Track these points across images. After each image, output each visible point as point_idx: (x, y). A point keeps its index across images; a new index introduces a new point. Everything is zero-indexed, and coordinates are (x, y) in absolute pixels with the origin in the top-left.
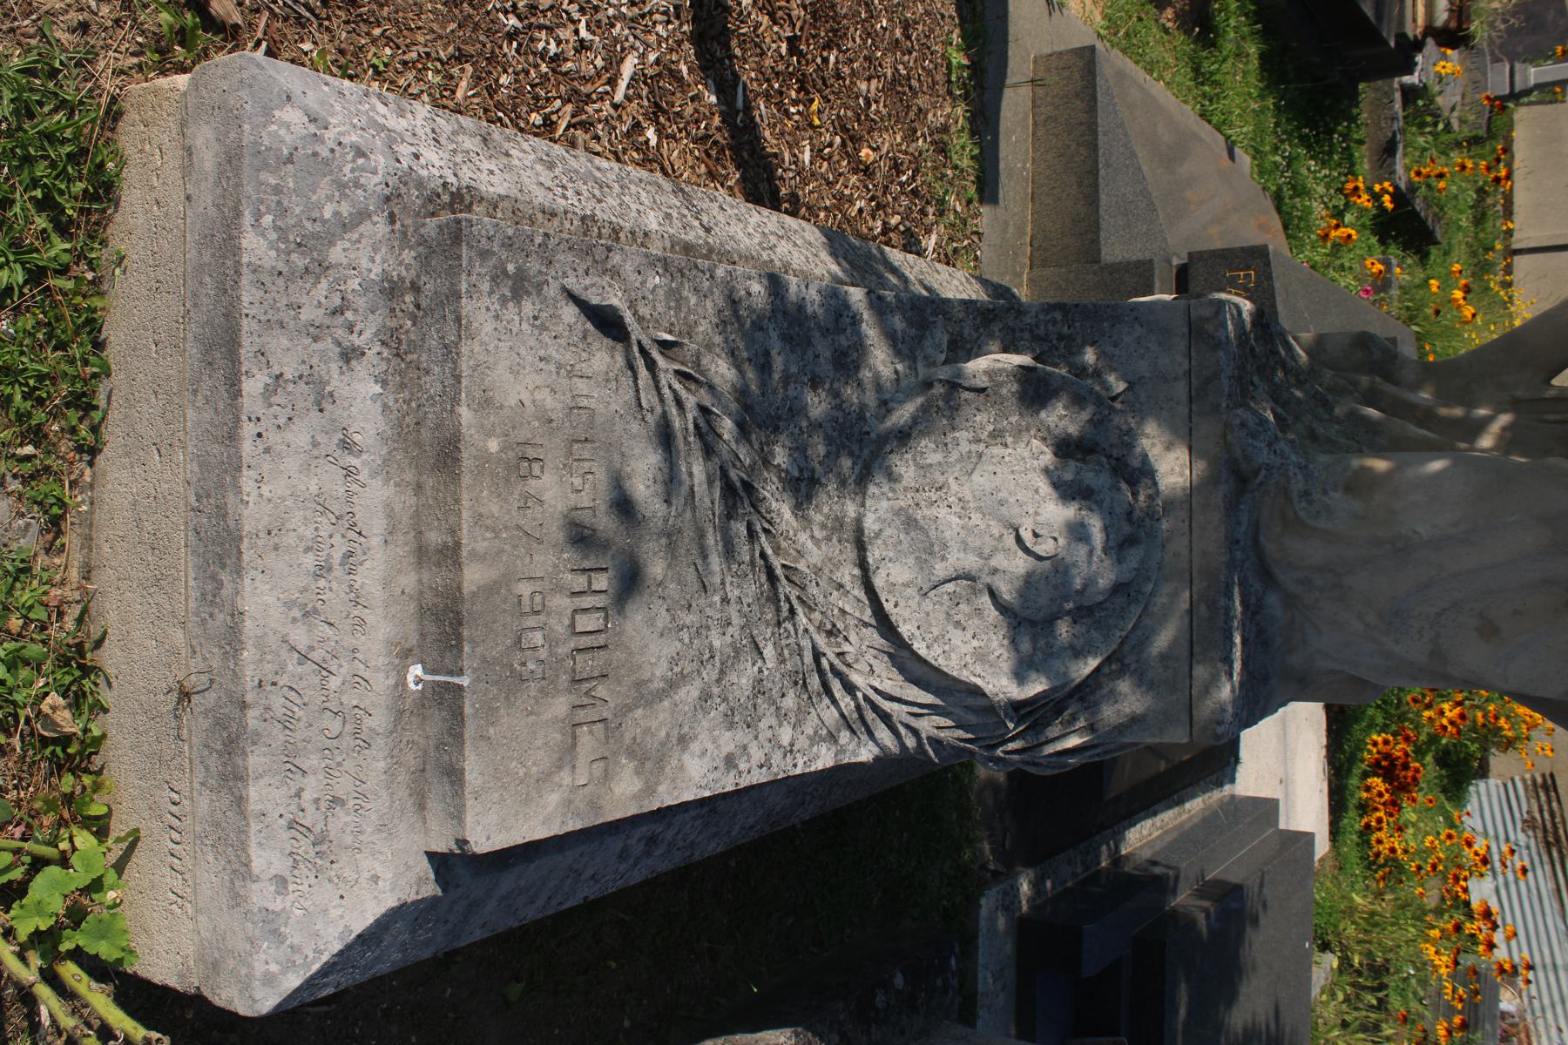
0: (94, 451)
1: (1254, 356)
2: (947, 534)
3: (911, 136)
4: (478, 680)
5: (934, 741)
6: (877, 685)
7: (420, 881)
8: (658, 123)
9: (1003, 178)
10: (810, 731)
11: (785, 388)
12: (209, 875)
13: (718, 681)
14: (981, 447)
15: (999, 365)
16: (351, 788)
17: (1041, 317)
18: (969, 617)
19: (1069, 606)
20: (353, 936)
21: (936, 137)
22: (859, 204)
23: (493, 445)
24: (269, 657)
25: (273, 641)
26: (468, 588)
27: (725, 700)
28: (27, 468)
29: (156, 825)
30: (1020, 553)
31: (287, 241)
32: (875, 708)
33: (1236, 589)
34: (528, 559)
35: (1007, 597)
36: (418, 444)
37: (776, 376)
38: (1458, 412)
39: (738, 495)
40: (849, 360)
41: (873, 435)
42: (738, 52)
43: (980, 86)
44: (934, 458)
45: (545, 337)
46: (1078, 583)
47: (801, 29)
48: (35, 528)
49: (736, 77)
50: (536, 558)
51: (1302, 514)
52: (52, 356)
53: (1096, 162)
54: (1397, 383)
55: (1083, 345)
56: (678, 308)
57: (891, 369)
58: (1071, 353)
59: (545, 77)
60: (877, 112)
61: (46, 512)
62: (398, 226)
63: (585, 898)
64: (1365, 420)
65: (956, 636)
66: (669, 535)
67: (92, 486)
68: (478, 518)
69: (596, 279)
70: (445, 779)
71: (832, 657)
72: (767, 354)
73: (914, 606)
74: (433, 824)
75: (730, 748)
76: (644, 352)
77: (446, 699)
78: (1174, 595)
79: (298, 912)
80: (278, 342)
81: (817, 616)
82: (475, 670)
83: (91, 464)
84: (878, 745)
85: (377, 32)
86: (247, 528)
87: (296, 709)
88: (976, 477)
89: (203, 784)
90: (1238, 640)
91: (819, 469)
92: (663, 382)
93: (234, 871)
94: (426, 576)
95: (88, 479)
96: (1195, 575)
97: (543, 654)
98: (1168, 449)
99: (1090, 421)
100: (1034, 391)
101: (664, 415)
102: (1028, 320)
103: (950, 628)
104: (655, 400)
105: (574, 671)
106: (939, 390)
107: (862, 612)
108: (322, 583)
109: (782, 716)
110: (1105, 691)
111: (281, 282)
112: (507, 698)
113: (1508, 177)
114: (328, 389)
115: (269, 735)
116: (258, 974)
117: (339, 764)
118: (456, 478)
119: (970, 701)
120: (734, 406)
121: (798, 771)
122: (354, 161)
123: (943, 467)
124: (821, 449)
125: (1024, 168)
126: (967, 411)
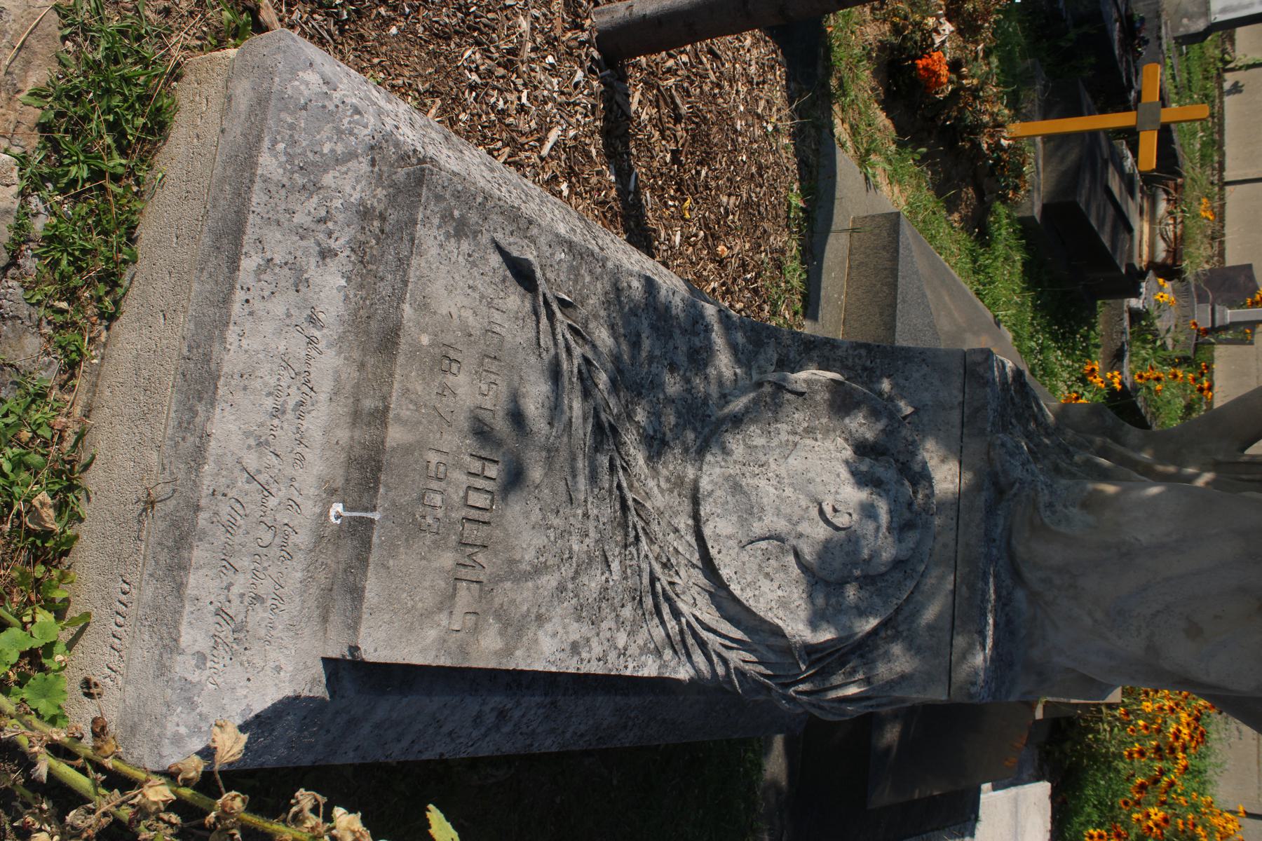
0: (112, 318)
1: (1014, 404)
2: (765, 500)
3: (756, 248)
4: (385, 518)
5: (741, 673)
6: (698, 614)
7: (314, 681)
8: (570, 182)
9: (822, 302)
10: (641, 642)
11: (650, 366)
12: (141, 651)
13: (573, 579)
14: (797, 438)
16: (271, 590)
19: (857, 573)
20: (252, 714)
21: (775, 255)
22: (713, 285)
23: (425, 340)
24: (224, 473)
25: (229, 460)
26: (389, 443)
27: (576, 596)
28: (59, 319)
29: (105, 612)
30: (822, 523)
31: (292, 164)
32: (695, 635)
33: (991, 580)
34: (438, 435)
35: (808, 558)
36: (367, 333)
37: (644, 354)
38: (1171, 469)
39: (605, 434)
40: (700, 358)
41: (713, 418)
42: (634, 151)
43: (811, 230)
44: (760, 441)
45: (475, 271)
46: (865, 553)
47: (683, 146)
48: (56, 366)
49: (631, 169)
50: (445, 436)
51: (1046, 520)
52: (96, 238)
53: (895, 298)
54: (1123, 445)
55: (881, 377)
56: (576, 282)
57: (732, 372)
59: (492, 124)
60: (733, 222)
61: (67, 356)
62: (376, 169)
63: (442, 754)
64: (1098, 465)
65: (765, 585)
66: (549, 451)
67: (105, 345)
68: (406, 391)
69: (518, 240)
70: (348, 596)
71: (665, 584)
72: (639, 335)
73: (734, 555)
74: (332, 634)
75: (575, 637)
76: (547, 304)
77: (359, 531)
78: (942, 578)
79: (210, 686)
80: (273, 236)
81: (656, 548)
82: (386, 510)
83: (108, 328)
84: (694, 667)
85: (376, 61)
86: (225, 369)
87: (238, 518)
88: (791, 460)
89: (151, 575)
90: (991, 621)
91: (669, 435)
92: (559, 330)
93: (164, 646)
94: (357, 434)
95: (103, 339)
96: (959, 562)
97: (440, 513)
98: (943, 461)
99: (883, 431)
100: (842, 402)
101: (557, 354)
102: (840, 353)
103: (761, 577)
104: (551, 344)
105: (462, 535)
106: (767, 389)
108: (276, 422)
109: (620, 622)
110: (881, 651)
111: (283, 192)
112: (407, 540)
113: (1210, 388)
114: (306, 276)
115: (214, 534)
116: (169, 734)
117: (265, 569)
118: (392, 357)
119: (772, 641)
120: (609, 365)
121: (628, 673)
122: (351, 116)
123: (766, 449)
124: (672, 420)
125: (839, 298)
126: (788, 409)
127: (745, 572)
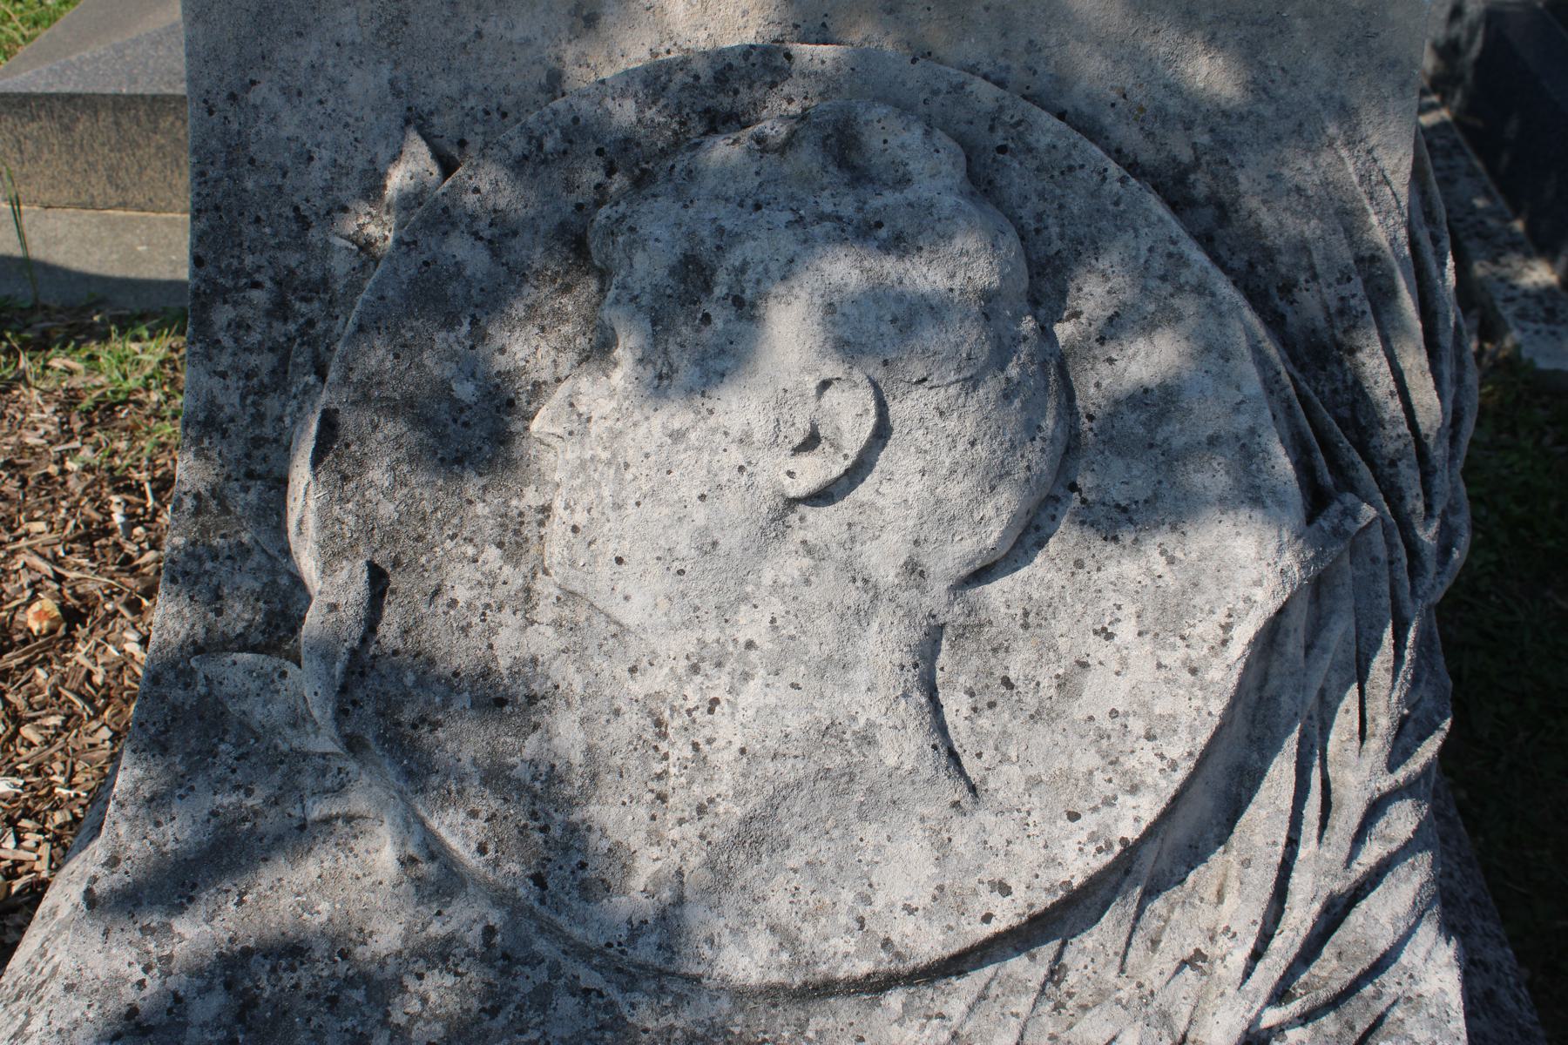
2: (795, 723)
14: (546, 588)
17: (225, 361)
18: (1047, 648)
21: (77, 425)
30: (863, 492)
35: (993, 534)
41: (495, 917)
58: (325, 283)
65: (1103, 692)
88: (631, 615)
102: (230, 400)
103: (1078, 711)
107: (1015, 987)
119: (1293, 646)
127: (1066, 775)
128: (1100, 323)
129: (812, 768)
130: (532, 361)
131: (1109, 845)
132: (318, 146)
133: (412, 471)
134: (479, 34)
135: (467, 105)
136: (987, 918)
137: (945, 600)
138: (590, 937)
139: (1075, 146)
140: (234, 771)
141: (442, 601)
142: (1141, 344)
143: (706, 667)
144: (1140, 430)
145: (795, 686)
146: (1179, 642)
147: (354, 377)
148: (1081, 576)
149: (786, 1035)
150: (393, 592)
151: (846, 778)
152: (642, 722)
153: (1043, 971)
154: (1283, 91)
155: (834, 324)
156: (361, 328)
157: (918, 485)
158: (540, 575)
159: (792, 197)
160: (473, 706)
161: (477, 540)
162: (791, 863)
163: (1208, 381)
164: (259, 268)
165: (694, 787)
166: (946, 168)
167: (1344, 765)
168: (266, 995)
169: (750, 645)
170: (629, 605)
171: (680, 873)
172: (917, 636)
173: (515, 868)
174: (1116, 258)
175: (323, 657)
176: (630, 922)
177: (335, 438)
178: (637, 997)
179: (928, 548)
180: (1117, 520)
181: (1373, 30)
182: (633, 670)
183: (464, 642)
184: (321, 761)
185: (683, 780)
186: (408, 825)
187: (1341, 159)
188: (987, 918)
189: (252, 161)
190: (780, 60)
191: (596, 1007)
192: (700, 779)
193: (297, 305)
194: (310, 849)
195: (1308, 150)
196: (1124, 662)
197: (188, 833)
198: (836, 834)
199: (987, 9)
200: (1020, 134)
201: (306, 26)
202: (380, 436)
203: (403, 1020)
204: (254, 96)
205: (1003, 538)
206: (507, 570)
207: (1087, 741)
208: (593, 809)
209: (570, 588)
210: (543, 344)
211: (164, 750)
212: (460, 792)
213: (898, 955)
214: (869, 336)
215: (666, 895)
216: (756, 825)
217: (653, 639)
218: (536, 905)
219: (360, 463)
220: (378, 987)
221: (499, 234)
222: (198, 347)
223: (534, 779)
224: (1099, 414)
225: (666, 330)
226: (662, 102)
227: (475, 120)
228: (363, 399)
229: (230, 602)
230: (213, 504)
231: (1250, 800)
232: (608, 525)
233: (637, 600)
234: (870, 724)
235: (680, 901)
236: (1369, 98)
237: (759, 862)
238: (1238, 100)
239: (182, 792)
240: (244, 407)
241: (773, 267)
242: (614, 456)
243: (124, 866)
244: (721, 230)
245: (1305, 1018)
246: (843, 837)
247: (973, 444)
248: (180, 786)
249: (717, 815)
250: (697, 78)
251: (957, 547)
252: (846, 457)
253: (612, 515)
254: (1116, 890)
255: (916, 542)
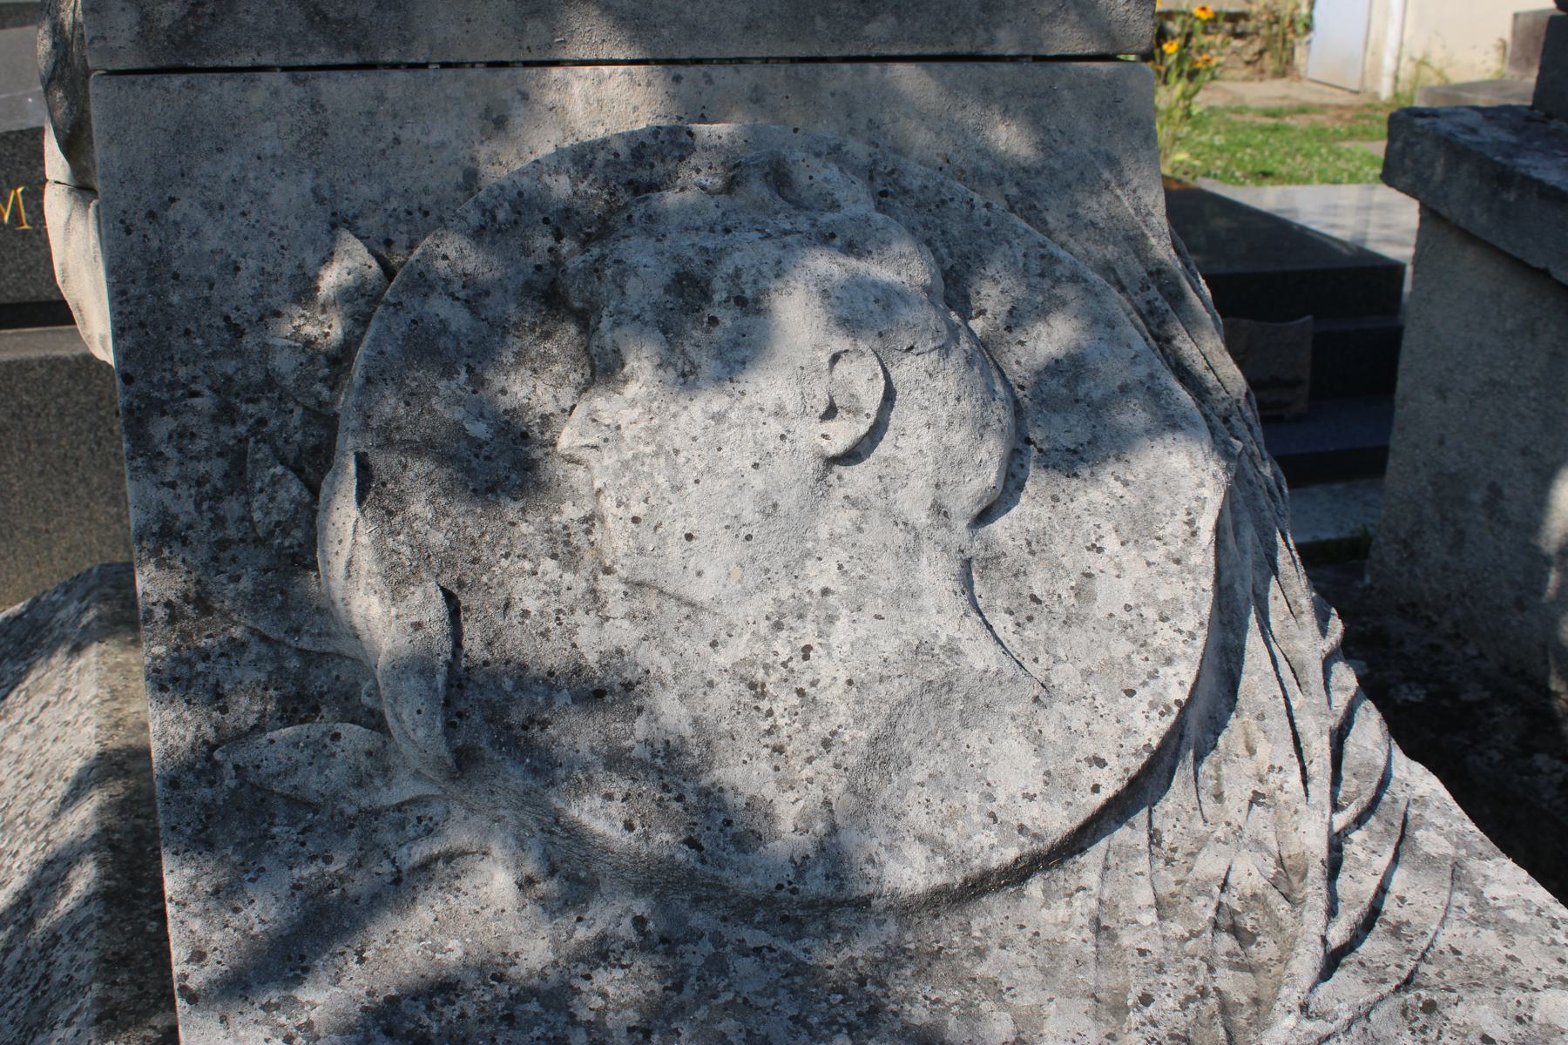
2: (889, 647)
6: (1295, 779)
10: (1489, 941)
14: (608, 585)
15: (366, 561)
17: (171, 472)
18: (1055, 567)
30: (884, 448)
35: (991, 475)
41: (641, 907)
65: (1112, 594)
71: (1314, 917)
81: (1227, 980)
88: (702, 592)
96: (799, 51)
102: (184, 507)
103: (1099, 610)
107: (1130, 853)
128: (1003, 316)
129: (917, 683)
130: (534, 399)
131: (1168, 709)
132: (244, 256)
133: (450, 503)
134: (397, 141)
135: (390, 207)
136: (1096, 789)
137: (967, 536)
138: (760, 883)
139: (942, 184)
140: (303, 844)
141: (515, 612)
142: (1040, 327)
143: (789, 621)
144: (1064, 391)
145: (878, 617)
146: (1157, 543)
147: (374, 423)
148: (1060, 507)
149: (956, 939)
150: (467, 609)
151: (945, 689)
152: (736, 688)
153: (1146, 836)
154: (1064, 148)
155: (832, 306)
156: (368, 380)
157: (927, 437)
158: (601, 576)
159: (754, 221)
160: (574, 701)
161: (531, 555)
162: (916, 778)
163: (1103, 346)
164: (194, 379)
165: (812, 727)
166: (863, 196)
167: (1291, 638)
168: (435, 1030)
169: (825, 592)
170: (702, 580)
171: (827, 803)
172: (956, 567)
173: (666, 837)
174: (999, 266)
175: (421, 672)
176: (792, 860)
177: (371, 478)
178: (807, 942)
179: (947, 490)
180: (1073, 460)
181: (1119, 96)
182: (714, 644)
183: (548, 646)
184: (397, 815)
185: (797, 725)
186: (521, 842)
187: (1118, 197)
188: (1096, 789)
189: (176, 276)
190: (684, 138)
191: (772, 960)
192: (816, 719)
193: (244, 407)
194: (414, 899)
195: (1092, 192)
196: (1119, 566)
197: (273, 911)
198: (946, 745)
199: (833, 95)
200: (895, 181)
201: (226, 142)
202: (412, 474)
203: (592, 1016)
204: (173, 214)
205: (998, 478)
206: (568, 577)
207: (1115, 633)
208: (718, 773)
209: (639, 578)
210: (539, 383)
211: (210, 845)
212: (589, 779)
213: (1035, 835)
214: (862, 314)
215: (820, 827)
216: (881, 745)
217: (728, 610)
218: (698, 866)
219: (399, 499)
220: (555, 996)
221: (473, 295)
222: (139, 462)
223: (654, 756)
224: (1026, 384)
225: (678, 335)
226: (591, 177)
227: (398, 220)
228: (387, 444)
229: (234, 698)
230: (189, 609)
231: (1240, 671)
232: (671, 508)
233: (710, 573)
234: (951, 639)
235: (834, 830)
236: (1125, 150)
237: (890, 781)
238: (1033, 158)
239: (251, 875)
240: (200, 513)
241: (765, 269)
242: (660, 446)
243: (212, 957)
244: (705, 250)
245: (1359, 821)
246: (952, 747)
247: (958, 399)
248: (247, 872)
249: (844, 743)
250: (616, 155)
251: (969, 487)
252: (868, 415)
253: (673, 497)
254: (1177, 756)
255: (937, 486)
